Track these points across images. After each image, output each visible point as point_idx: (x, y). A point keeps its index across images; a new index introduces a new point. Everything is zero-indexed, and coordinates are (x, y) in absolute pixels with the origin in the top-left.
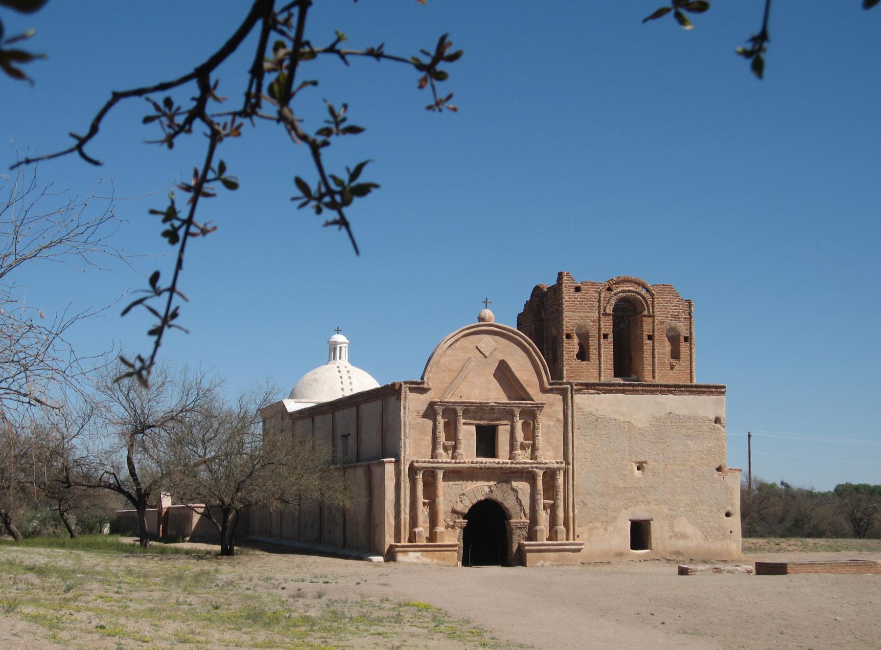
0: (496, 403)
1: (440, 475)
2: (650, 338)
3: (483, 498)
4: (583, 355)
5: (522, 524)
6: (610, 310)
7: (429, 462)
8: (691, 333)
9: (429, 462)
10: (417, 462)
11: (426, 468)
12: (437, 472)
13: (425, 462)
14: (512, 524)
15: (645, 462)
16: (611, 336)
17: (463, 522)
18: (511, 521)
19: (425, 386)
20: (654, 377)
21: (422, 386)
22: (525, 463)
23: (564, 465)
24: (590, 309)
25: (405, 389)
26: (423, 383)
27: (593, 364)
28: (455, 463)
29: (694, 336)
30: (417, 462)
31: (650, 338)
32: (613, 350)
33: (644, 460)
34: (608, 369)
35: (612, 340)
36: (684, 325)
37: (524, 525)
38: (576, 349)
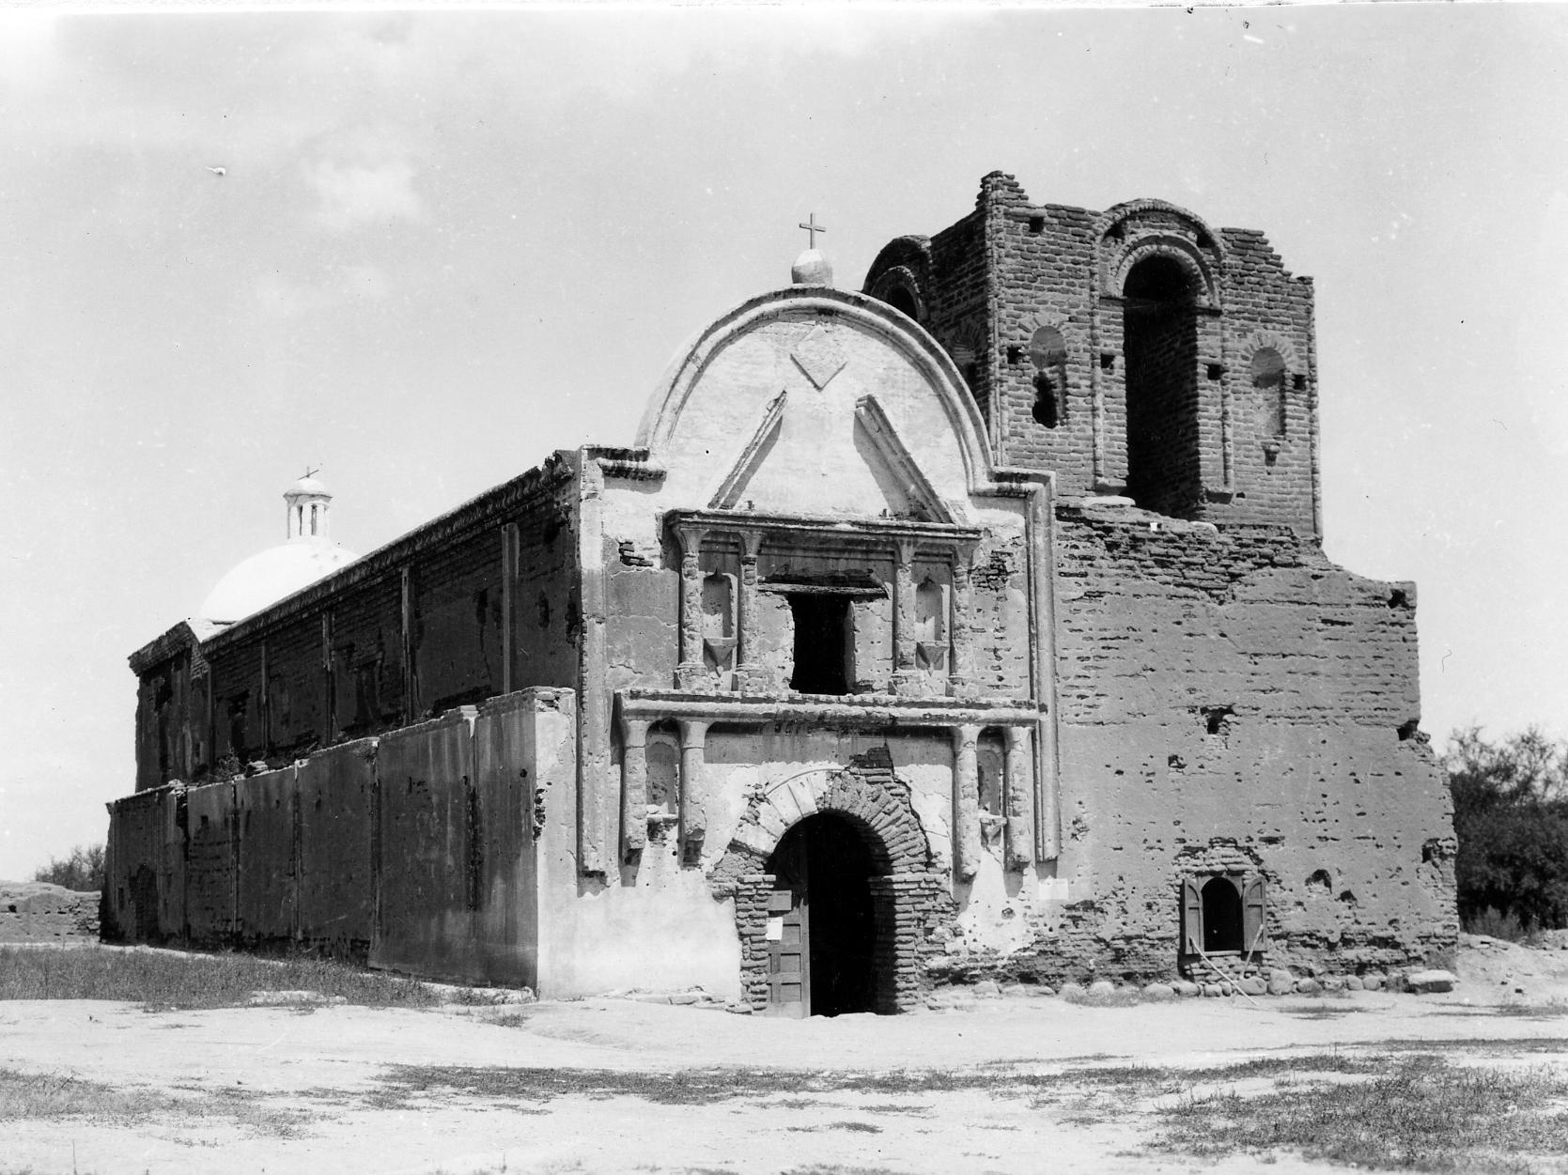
0: (853, 524)
1: (697, 731)
2: (1215, 372)
3: (814, 809)
4: (1046, 412)
5: (923, 885)
6: (1116, 287)
7: (668, 697)
8: (1312, 366)
9: (668, 697)
10: (635, 695)
11: (657, 713)
12: (688, 727)
13: (655, 697)
14: (895, 886)
15: (1229, 711)
16: (1119, 361)
17: (765, 882)
18: (894, 878)
19: (651, 464)
20: (1226, 482)
21: (641, 465)
22: (934, 705)
23: (1033, 713)
24: (1068, 284)
25: (592, 473)
26: (644, 455)
27: (1077, 438)
28: (745, 700)
29: (1322, 374)
30: (635, 695)
31: (1215, 372)
32: (1124, 400)
33: (1226, 703)
34: (1114, 453)
35: (1123, 372)
36: (1295, 343)
37: (930, 889)
38: (1029, 396)
